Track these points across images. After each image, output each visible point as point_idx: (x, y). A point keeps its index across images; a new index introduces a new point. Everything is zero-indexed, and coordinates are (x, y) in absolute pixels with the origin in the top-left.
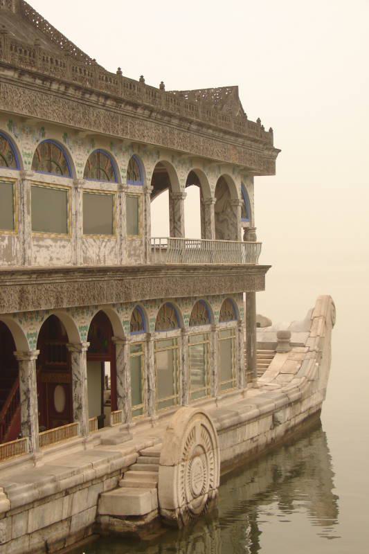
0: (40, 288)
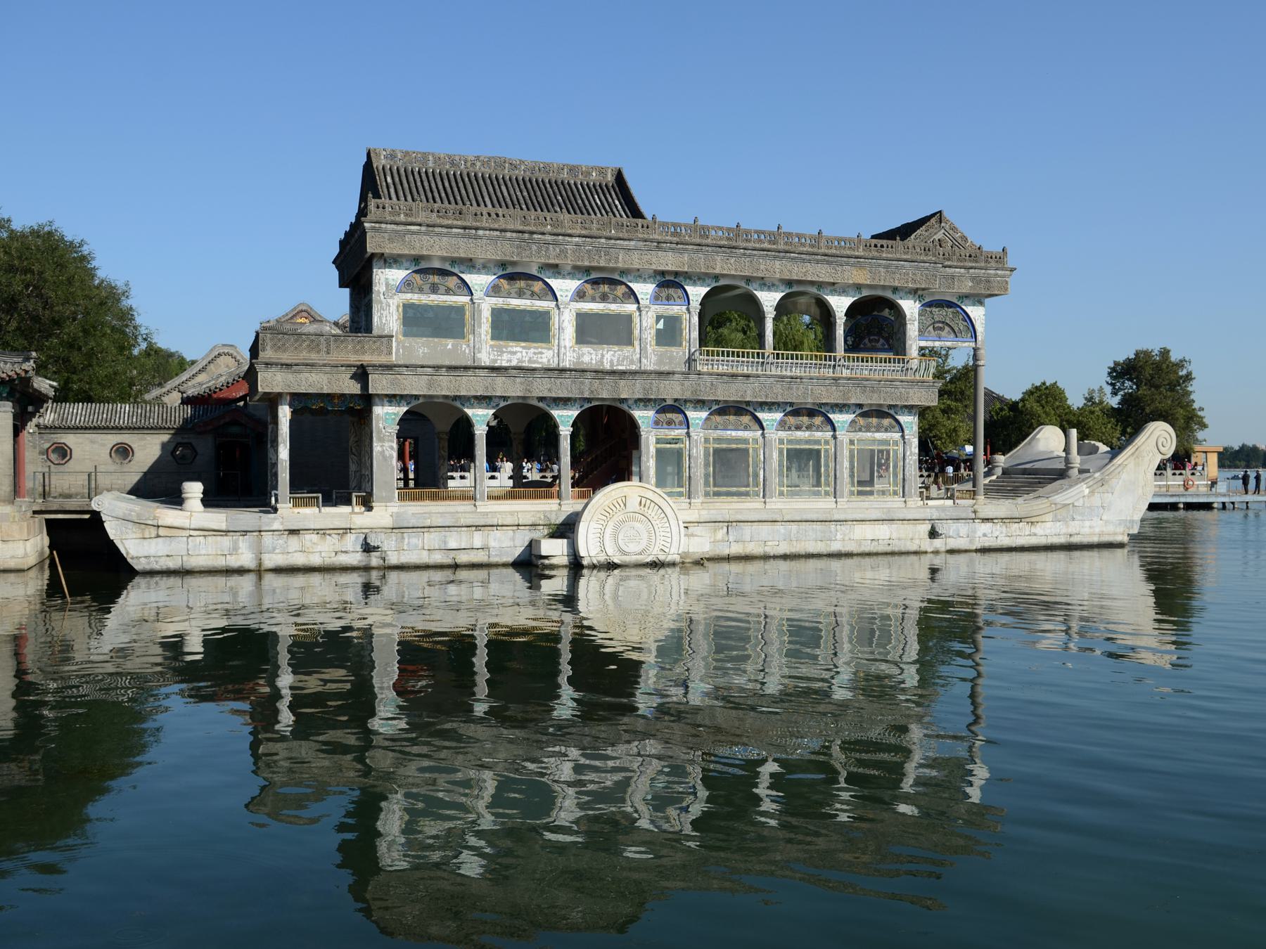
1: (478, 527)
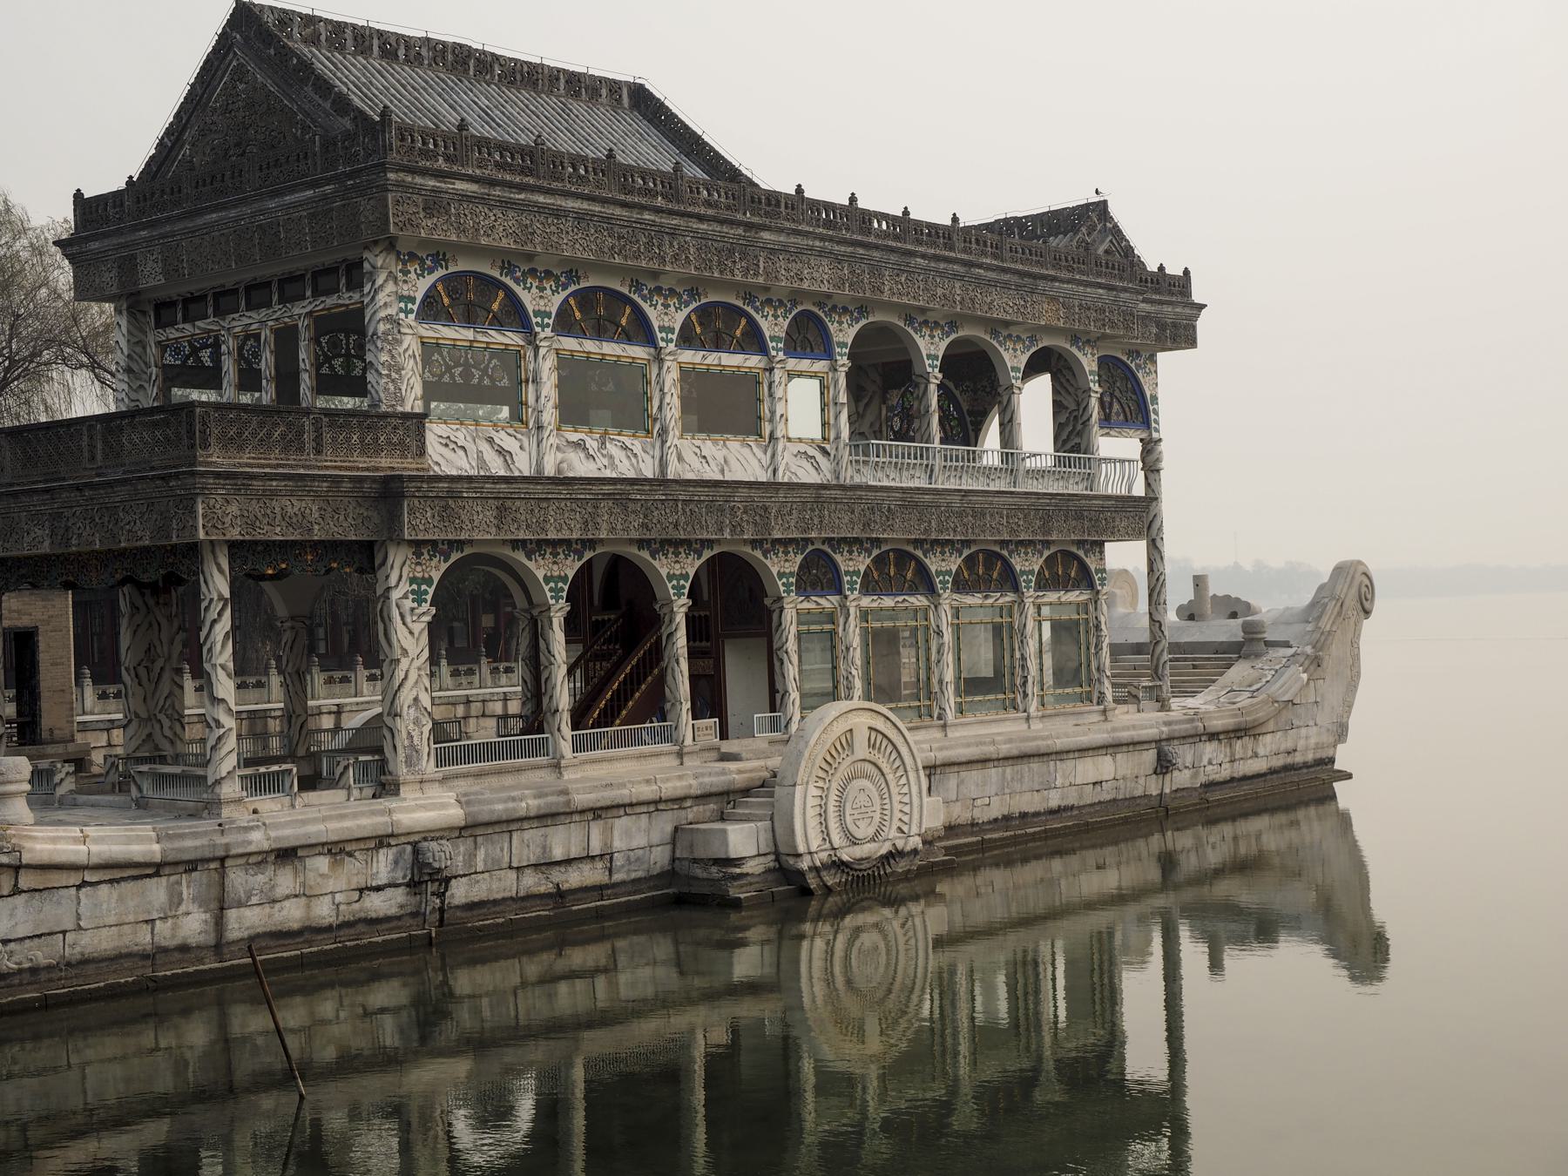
0: (544, 505)
1: (598, 812)
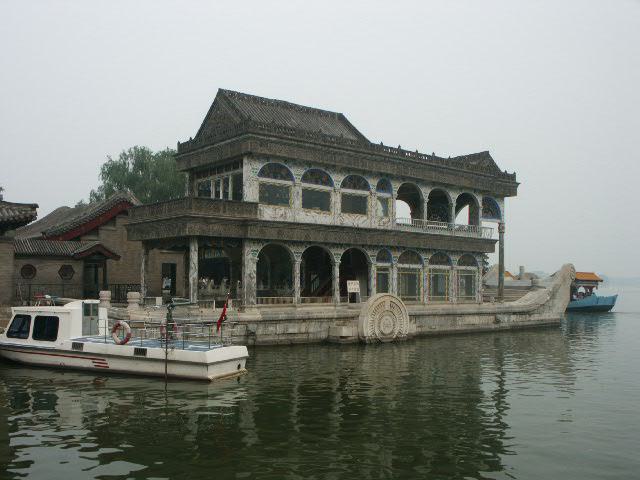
1: (304, 320)
